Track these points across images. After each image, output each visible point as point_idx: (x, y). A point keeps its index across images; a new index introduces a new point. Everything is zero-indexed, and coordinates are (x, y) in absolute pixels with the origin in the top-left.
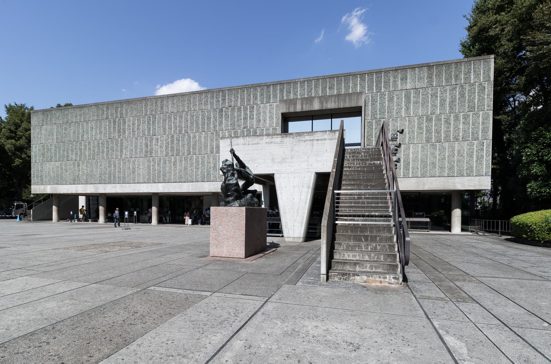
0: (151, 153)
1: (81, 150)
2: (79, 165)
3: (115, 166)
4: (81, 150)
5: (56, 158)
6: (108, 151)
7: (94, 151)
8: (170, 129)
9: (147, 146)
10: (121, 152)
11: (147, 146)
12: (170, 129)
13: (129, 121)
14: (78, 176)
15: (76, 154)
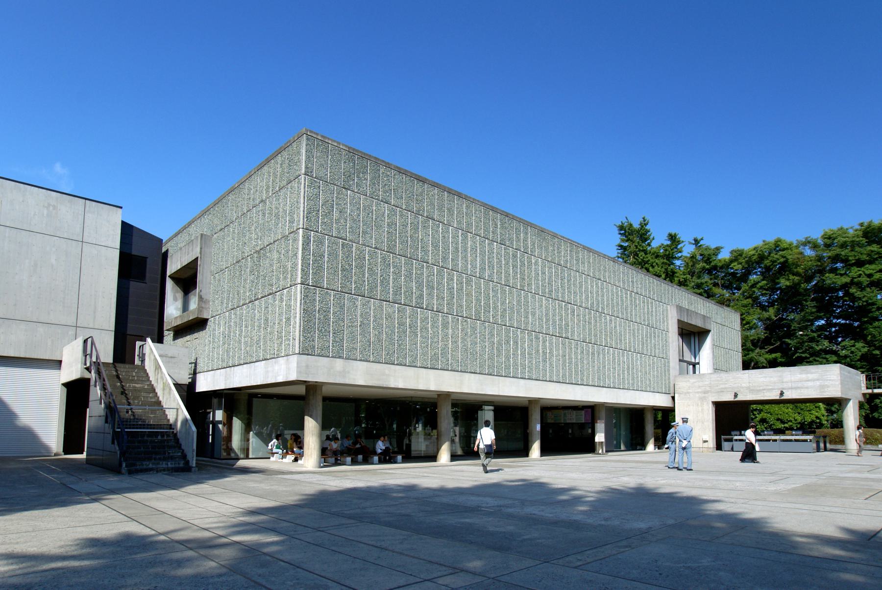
0: (567, 331)
1: (451, 289)
2: (445, 325)
3: (516, 343)
4: (451, 289)
5: (385, 290)
6: (505, 310)
7: (478, 300)
8: (587, 299)
9: (561, 320)
10: (527, 317)
11: (561, 320)
12: (587, 299)
13: (536, 263)
14: (444, 353)
15: (440, 298)
